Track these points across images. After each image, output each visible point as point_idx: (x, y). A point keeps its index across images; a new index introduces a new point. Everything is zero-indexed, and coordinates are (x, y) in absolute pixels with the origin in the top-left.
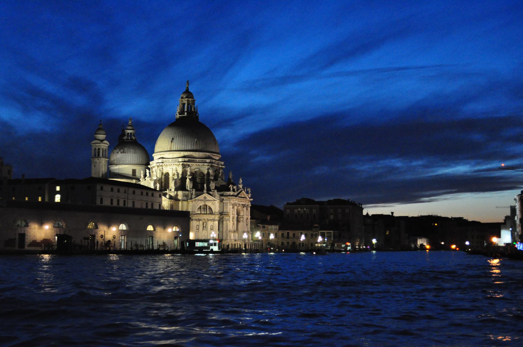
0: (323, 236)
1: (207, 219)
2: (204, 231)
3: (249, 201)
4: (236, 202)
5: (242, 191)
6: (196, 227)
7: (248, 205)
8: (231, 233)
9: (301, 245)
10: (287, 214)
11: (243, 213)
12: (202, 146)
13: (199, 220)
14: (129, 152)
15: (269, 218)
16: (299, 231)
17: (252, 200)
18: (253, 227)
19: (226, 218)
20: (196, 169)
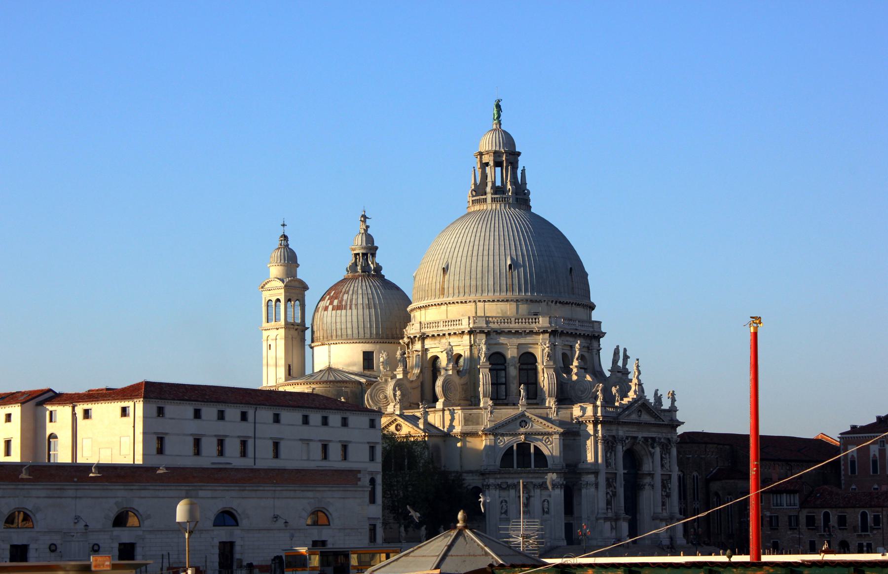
4: (621, 433)
11: (653, 462)
14: (353, 307)
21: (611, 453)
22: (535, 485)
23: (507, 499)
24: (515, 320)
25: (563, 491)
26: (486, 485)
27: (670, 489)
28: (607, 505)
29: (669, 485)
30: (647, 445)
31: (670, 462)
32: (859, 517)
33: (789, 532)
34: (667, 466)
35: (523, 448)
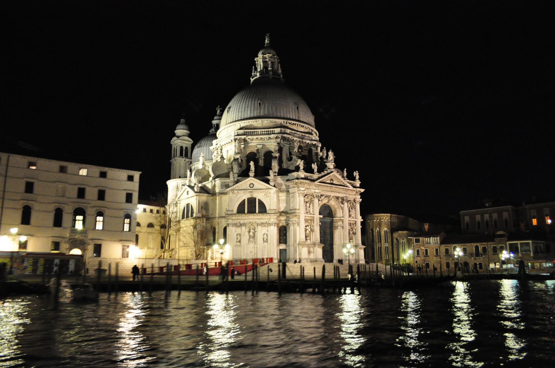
0: (513, 249)
1: (256, 222)
2: (252, 245)
3: (357, 192)
4: (317, 191)
5: (332, 172)
6: (236, 237)
7: (355, 201)
8: (301, 247)
9: (478, 266)
10: (466, 222)
11: (343, 212)
12: (268, 111)
13: (241, 225)
14: (205, 145)
15: (426, 227)
16: (473, 244)
17: (363, 190)
18: (405, 242)
19: (294, 219)
20: (257, 146)
21: (310, 204)
22: (258, 224)
23: (240, 233)
24: (261, 131)
25: (276, 227)
26: (227, 224)
27: (355, 230)
28: (306, 237)
29: (355, 227)
30: (339, 202)
31: (355, 213)
32: (474, 248)
33: (435, 258)
34: (353, 215)
35: (252, 201)
